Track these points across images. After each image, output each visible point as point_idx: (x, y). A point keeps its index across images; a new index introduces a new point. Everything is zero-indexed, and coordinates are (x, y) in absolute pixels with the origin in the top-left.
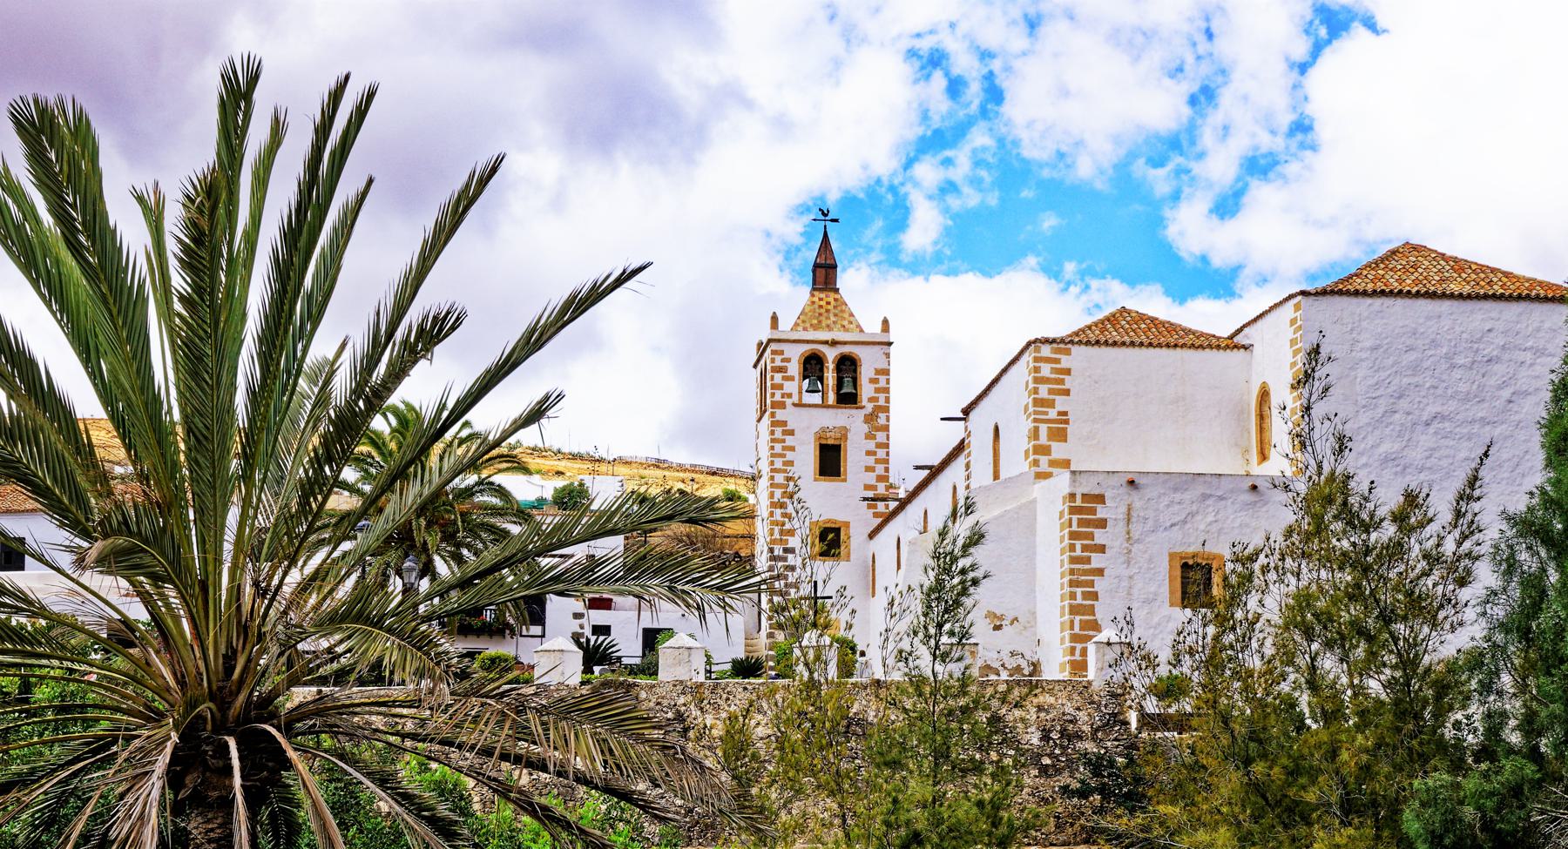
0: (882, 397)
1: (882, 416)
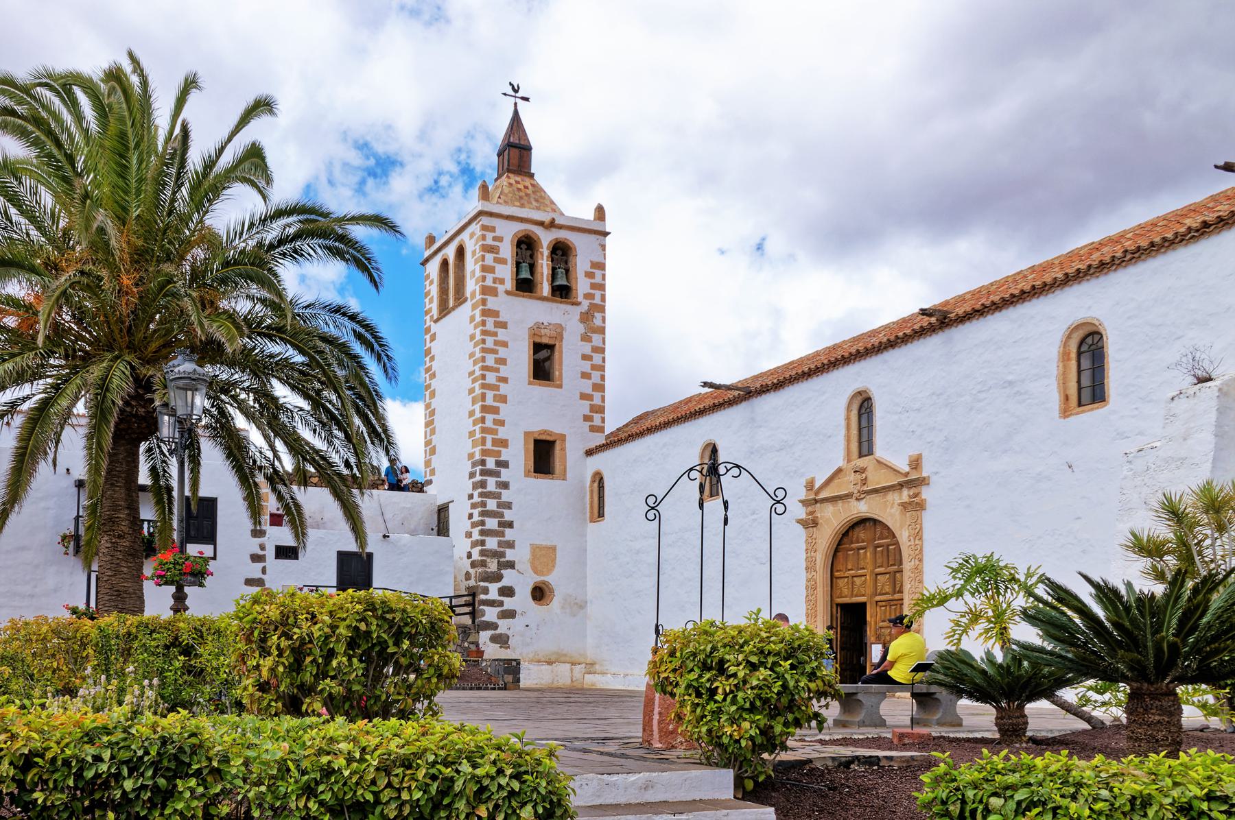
0: (598, 293)
1: (598, 315)
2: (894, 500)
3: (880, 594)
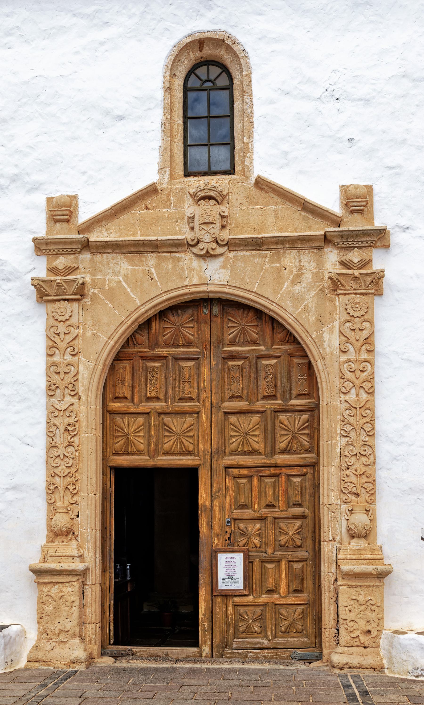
2: (301, 267)
3: (234, 453)
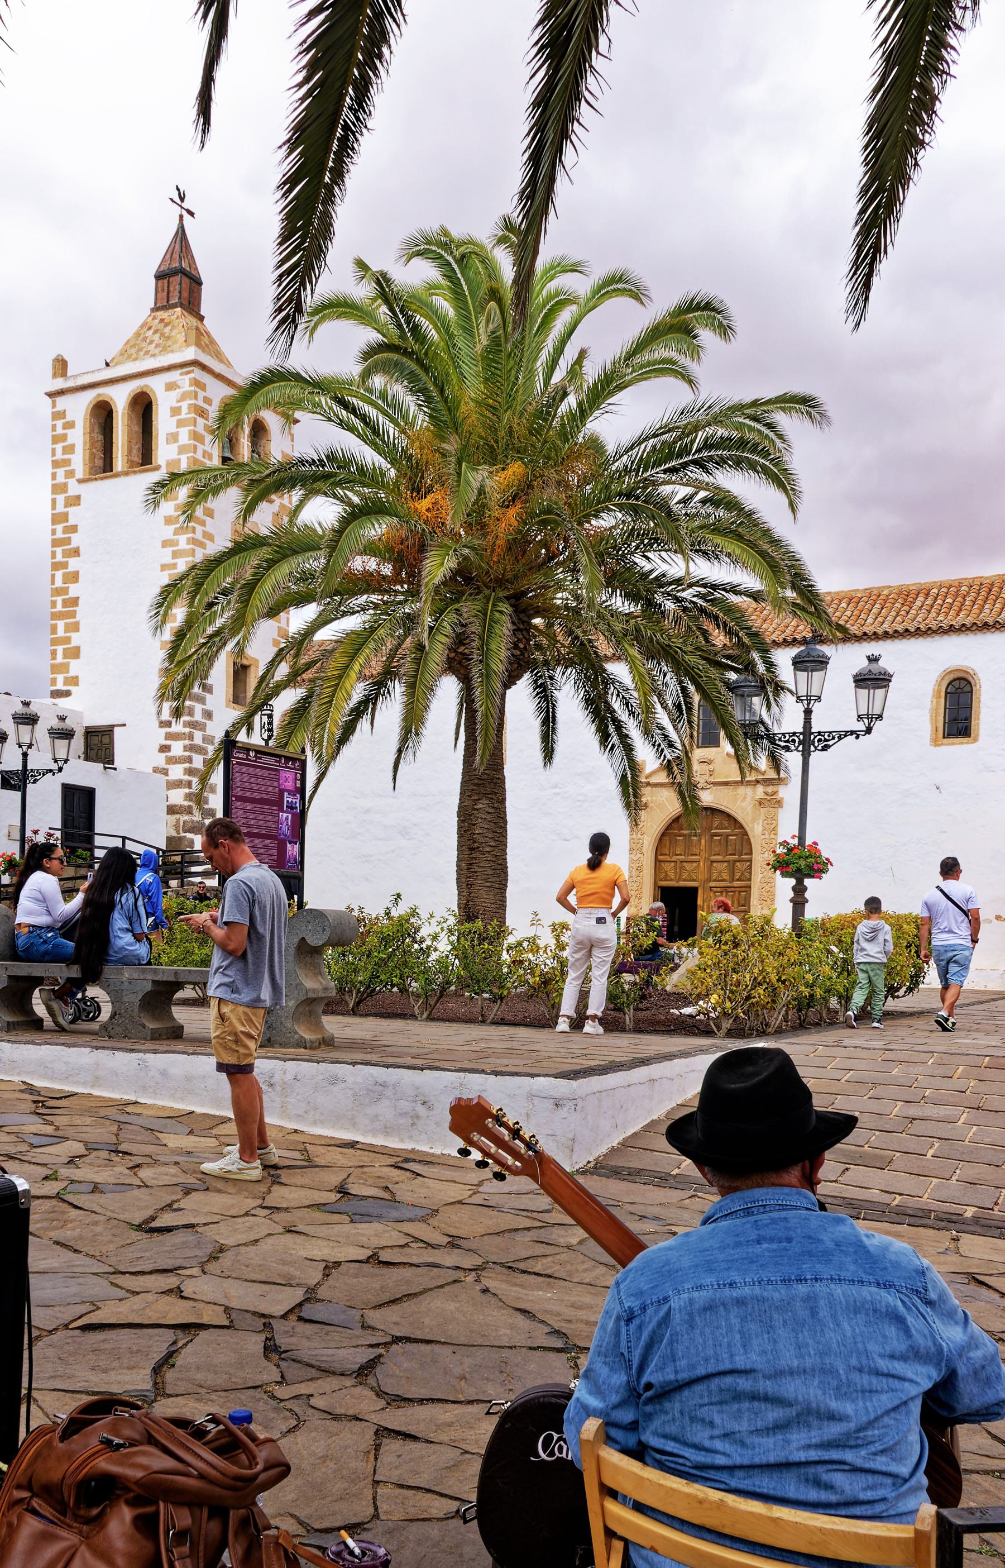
3: (715, 881)
